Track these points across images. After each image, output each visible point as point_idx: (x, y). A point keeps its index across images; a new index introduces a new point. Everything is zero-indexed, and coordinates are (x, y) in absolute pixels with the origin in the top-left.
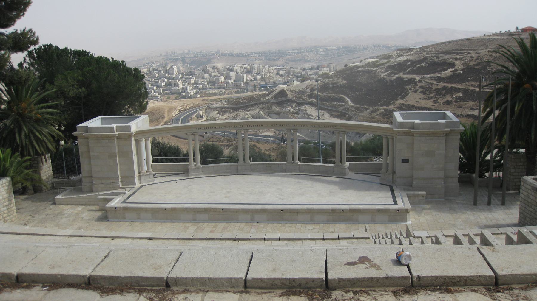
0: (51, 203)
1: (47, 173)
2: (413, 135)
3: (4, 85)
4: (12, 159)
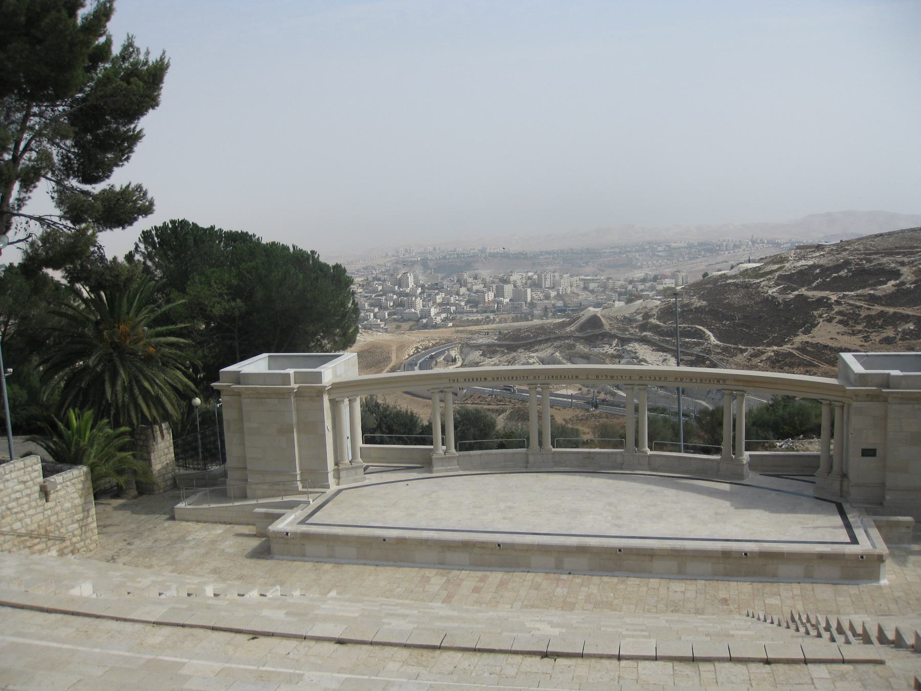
0: (167, 516)
1: (163, 459)
2: (886, 400)
3: (87, 288)
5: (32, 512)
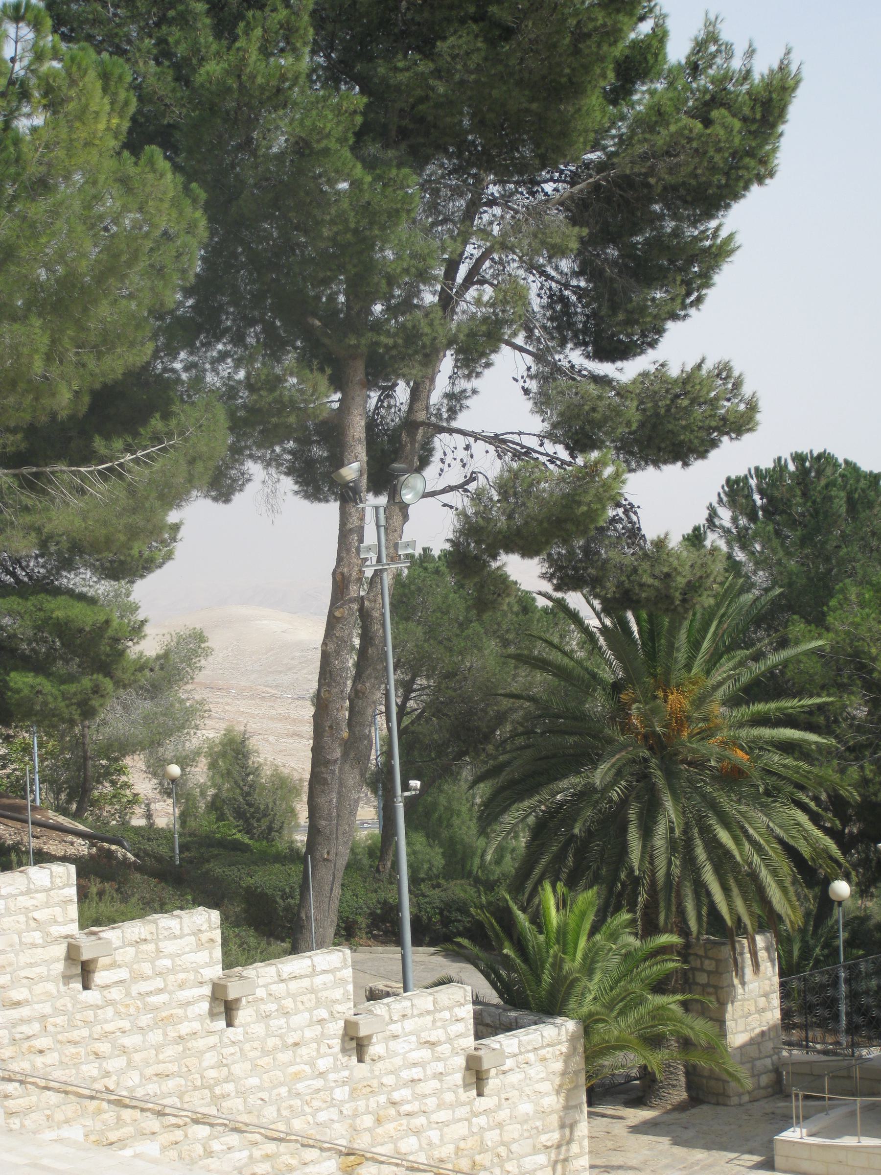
0: (757, 1158)
3: (597, 603)
4: (598, 937)
5: (443, 1116)
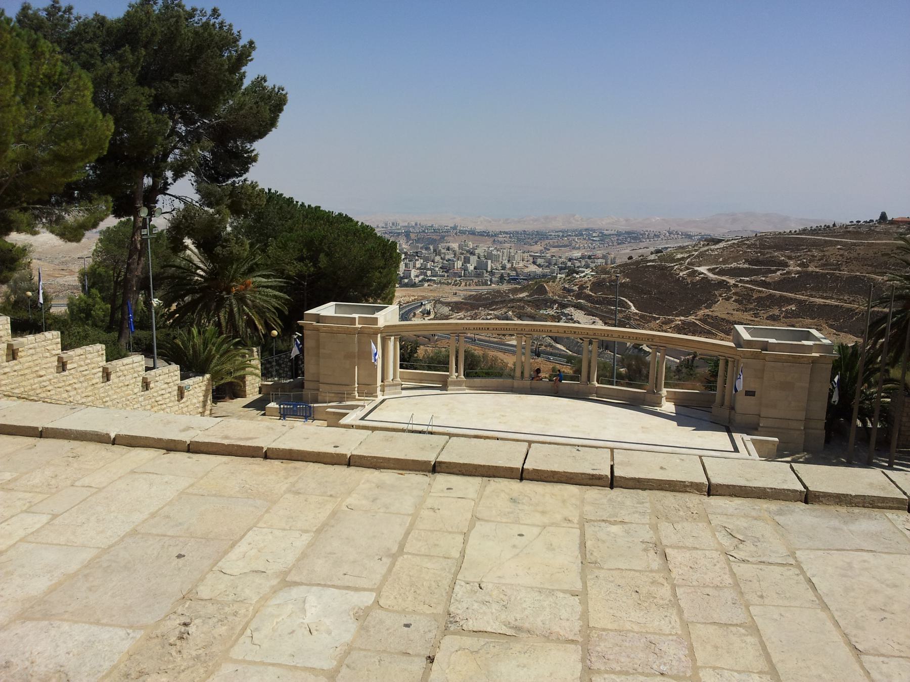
5: (171, 404)
